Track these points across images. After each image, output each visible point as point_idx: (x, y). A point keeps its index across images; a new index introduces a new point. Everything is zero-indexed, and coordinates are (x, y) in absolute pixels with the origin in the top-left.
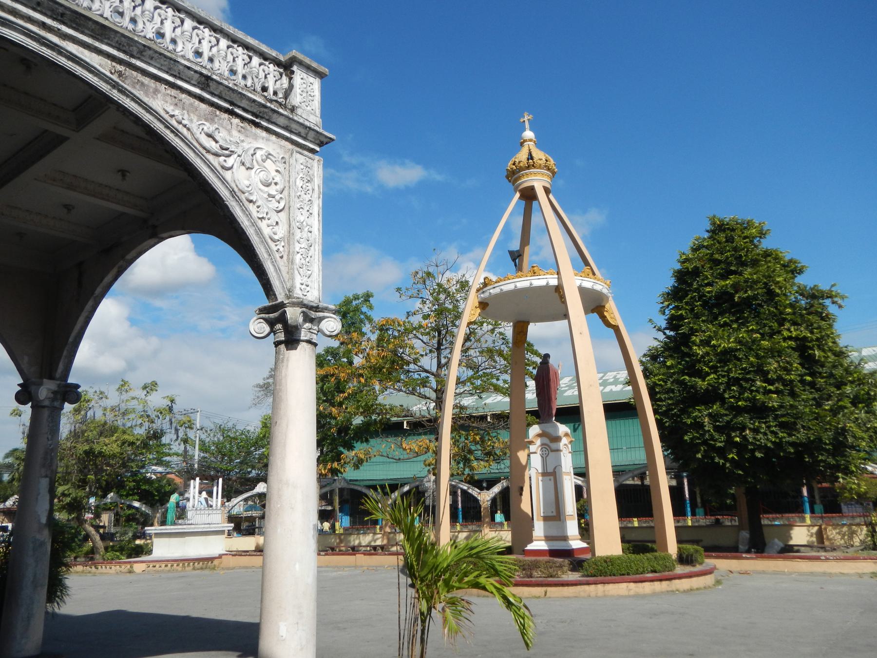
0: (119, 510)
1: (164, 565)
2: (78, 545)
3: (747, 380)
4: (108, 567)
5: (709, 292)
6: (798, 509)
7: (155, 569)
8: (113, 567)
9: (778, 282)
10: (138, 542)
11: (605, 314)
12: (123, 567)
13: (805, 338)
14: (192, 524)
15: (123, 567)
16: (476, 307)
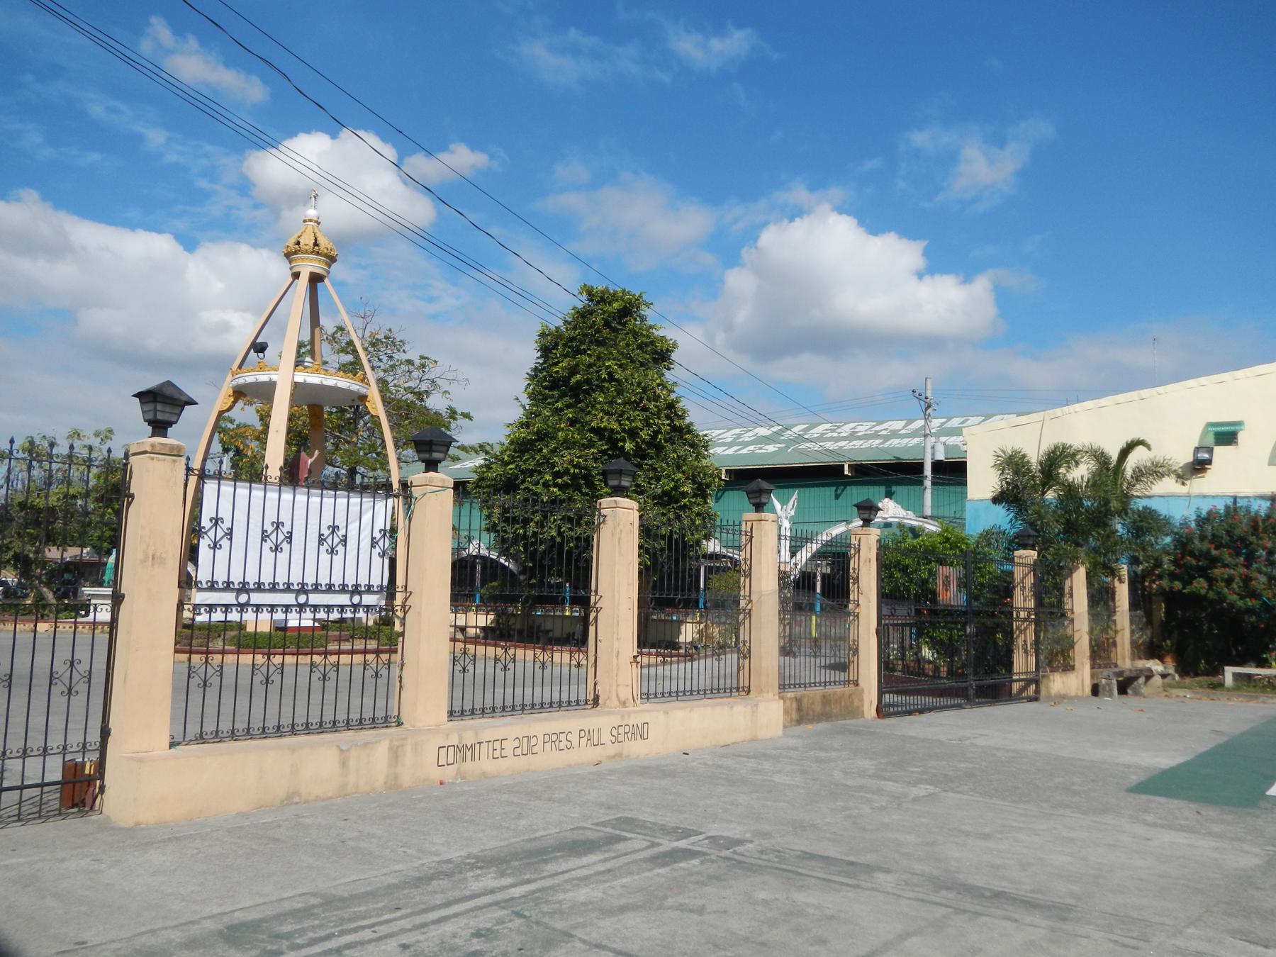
1: (67, 627)
3: (540, 473)
5: (557, 372)
6: (691, 604)
9: (609, 367)
11: (367, 404)
13: (612, 430)
16: (230, 396)
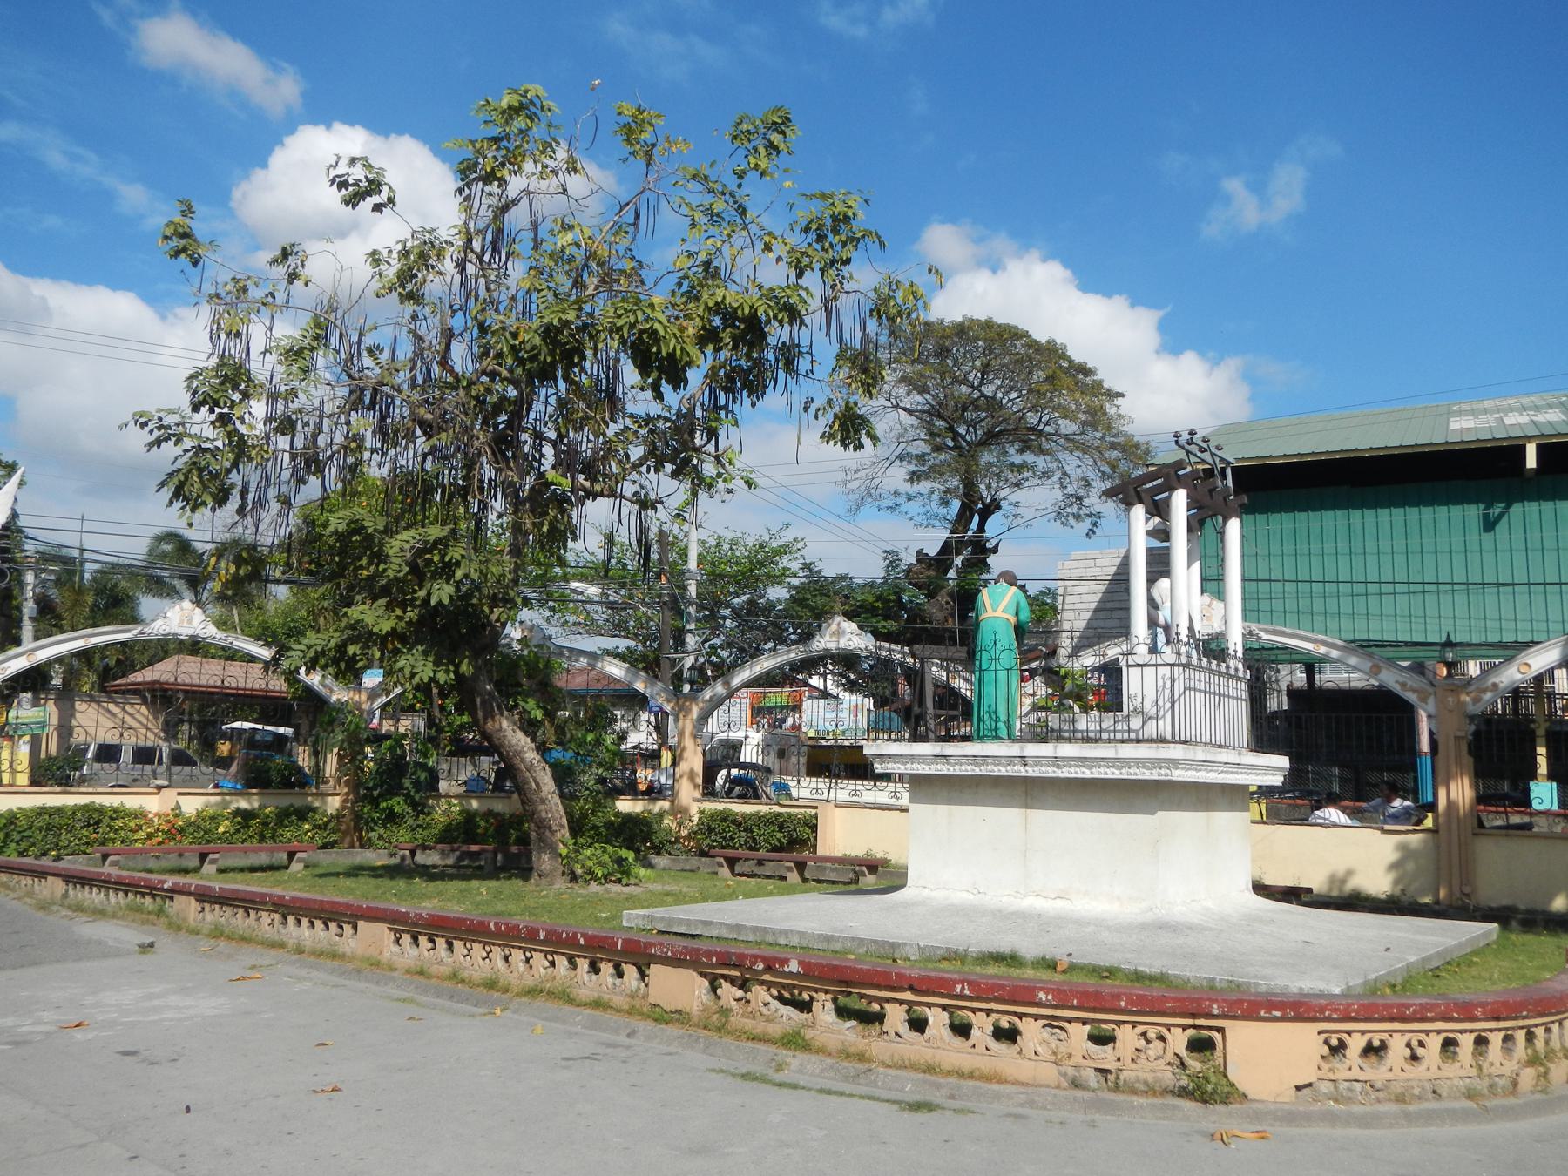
0: (437, 713)
2: (414, 804)
4: (982, 1026)
7: (1377, 1073)
8: (1032, 1031)
10: (625, 805)
12: (1127, 1037)
14: (1162, 740)
15: (1127, 1037)
